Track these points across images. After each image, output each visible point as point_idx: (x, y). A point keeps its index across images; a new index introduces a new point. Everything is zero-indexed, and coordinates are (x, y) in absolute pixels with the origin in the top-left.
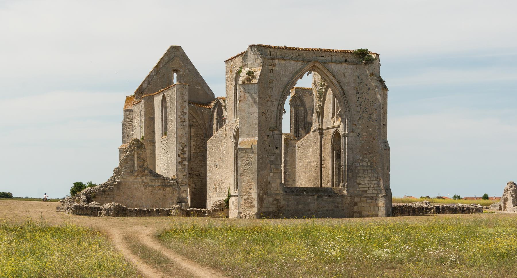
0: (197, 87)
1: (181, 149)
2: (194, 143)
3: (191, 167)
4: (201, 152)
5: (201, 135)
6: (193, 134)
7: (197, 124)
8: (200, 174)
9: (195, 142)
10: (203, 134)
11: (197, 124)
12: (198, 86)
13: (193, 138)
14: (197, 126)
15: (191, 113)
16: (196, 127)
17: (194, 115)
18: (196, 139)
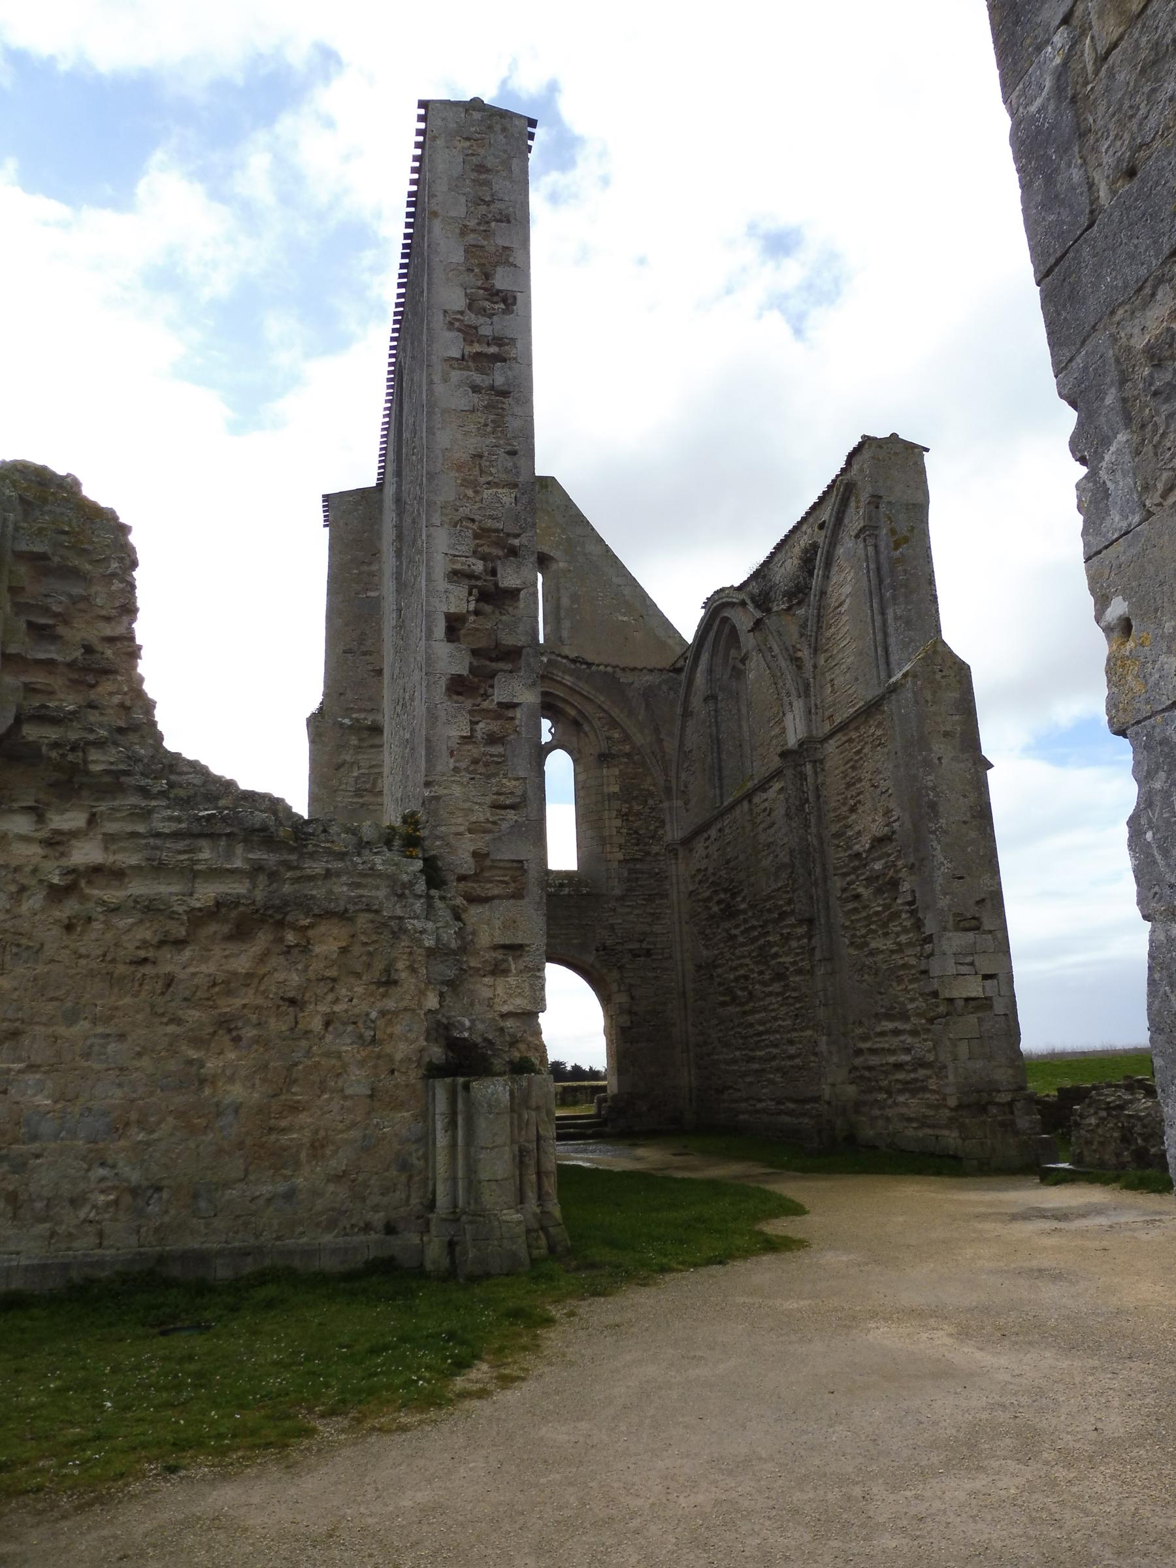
0: (620, 618)
1: (471, 576)
2: (618, 822)
3: (611, 922)
4: (648, 858)
5: (648, 790)
6: (616, 789)
7: (627, 748)
8: (648, 950)
9: (625, 817)
10: (654, 785)
11: (628, 747)
12: (624, 615)
13: (616, 804)
14: (628, 755)
15: (600, 707)
16: (626, 760)
17: (615, 712)
18: (627, 806)
